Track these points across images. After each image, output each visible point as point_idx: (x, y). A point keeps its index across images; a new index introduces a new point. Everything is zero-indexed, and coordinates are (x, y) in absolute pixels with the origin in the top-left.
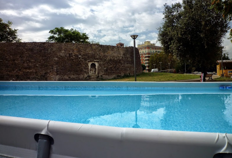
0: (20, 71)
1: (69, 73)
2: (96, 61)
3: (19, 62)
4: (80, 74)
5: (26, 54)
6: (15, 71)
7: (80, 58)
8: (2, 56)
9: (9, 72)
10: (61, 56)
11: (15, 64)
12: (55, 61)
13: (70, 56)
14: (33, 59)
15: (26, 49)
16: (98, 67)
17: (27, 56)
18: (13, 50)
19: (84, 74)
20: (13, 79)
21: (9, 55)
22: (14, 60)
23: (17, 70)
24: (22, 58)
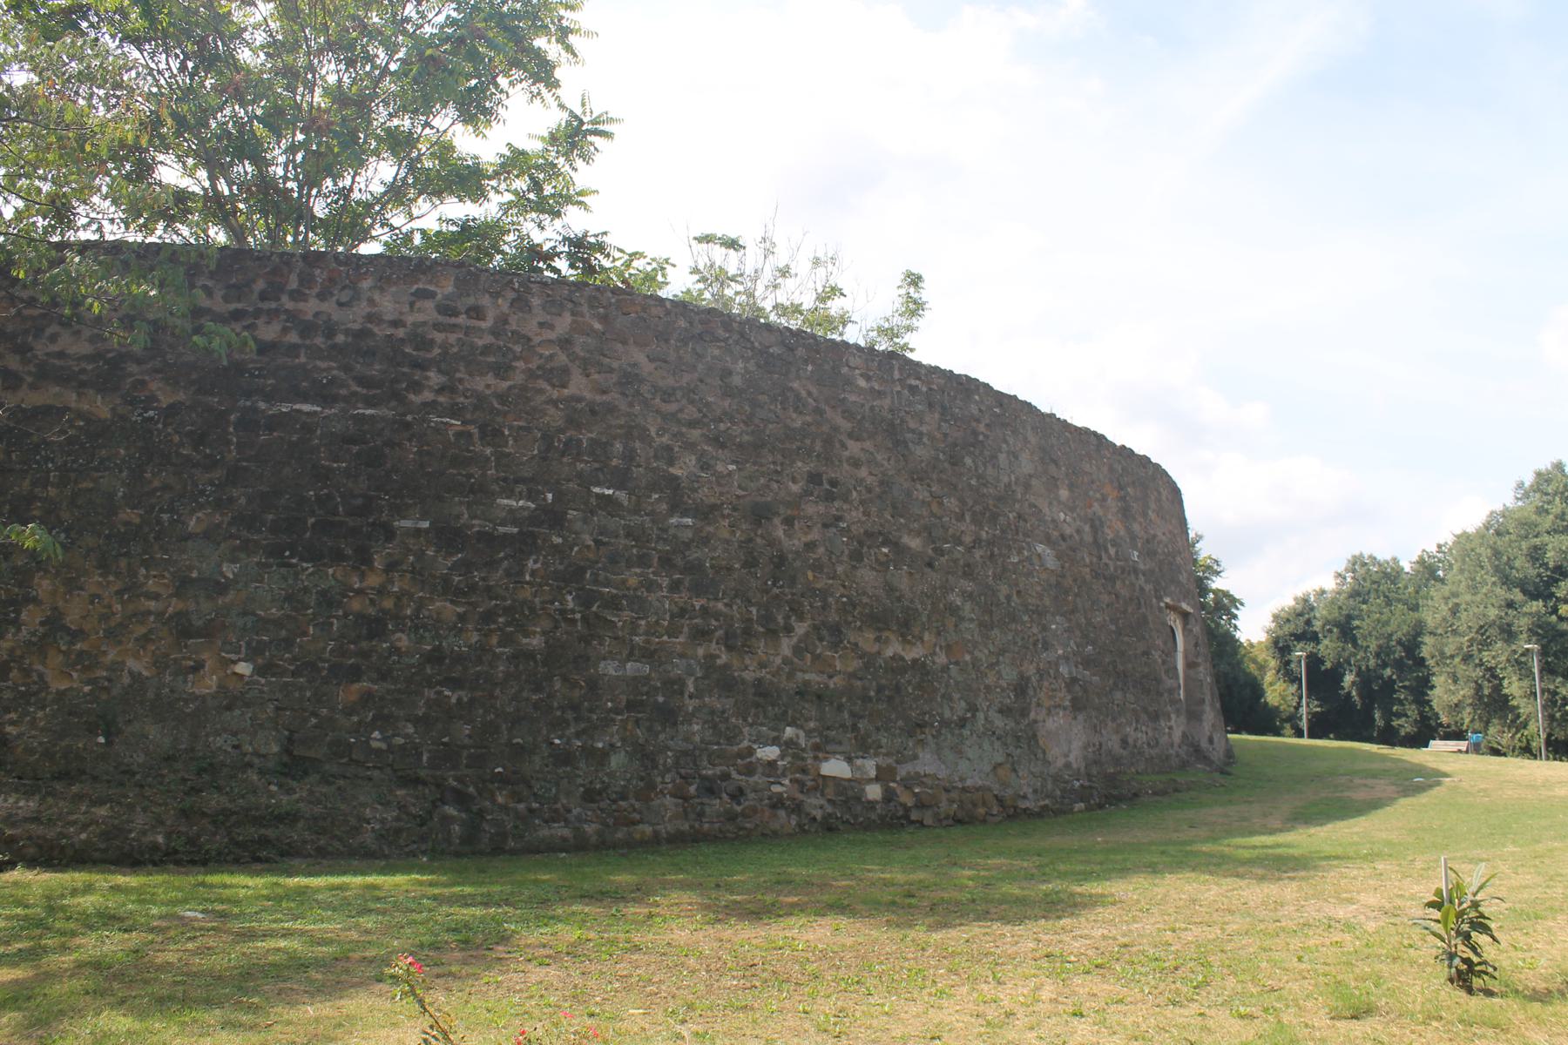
0: (835, 646)
1: (1118, 695)
2: (1184, 606)
3: (810, 546)
4: (1155, 717)
5: (856, 463)
6: (786, 646)
7: (1136, 571)
8: (618, 446)
9: (730, 648)
10: (1063, 537)
11: (780, 561)
12: (1044, 576)
13: (1095, 541)
14: (919, 534)
15: (848, 414)
16: (1190, 665)
17: (869, 490)
18: (728, 392)
19: (1169, 719)
20: (789, 732)
21: (690, 446)
22: (760, 515)
23: (801, 628)
24: (829, 497)
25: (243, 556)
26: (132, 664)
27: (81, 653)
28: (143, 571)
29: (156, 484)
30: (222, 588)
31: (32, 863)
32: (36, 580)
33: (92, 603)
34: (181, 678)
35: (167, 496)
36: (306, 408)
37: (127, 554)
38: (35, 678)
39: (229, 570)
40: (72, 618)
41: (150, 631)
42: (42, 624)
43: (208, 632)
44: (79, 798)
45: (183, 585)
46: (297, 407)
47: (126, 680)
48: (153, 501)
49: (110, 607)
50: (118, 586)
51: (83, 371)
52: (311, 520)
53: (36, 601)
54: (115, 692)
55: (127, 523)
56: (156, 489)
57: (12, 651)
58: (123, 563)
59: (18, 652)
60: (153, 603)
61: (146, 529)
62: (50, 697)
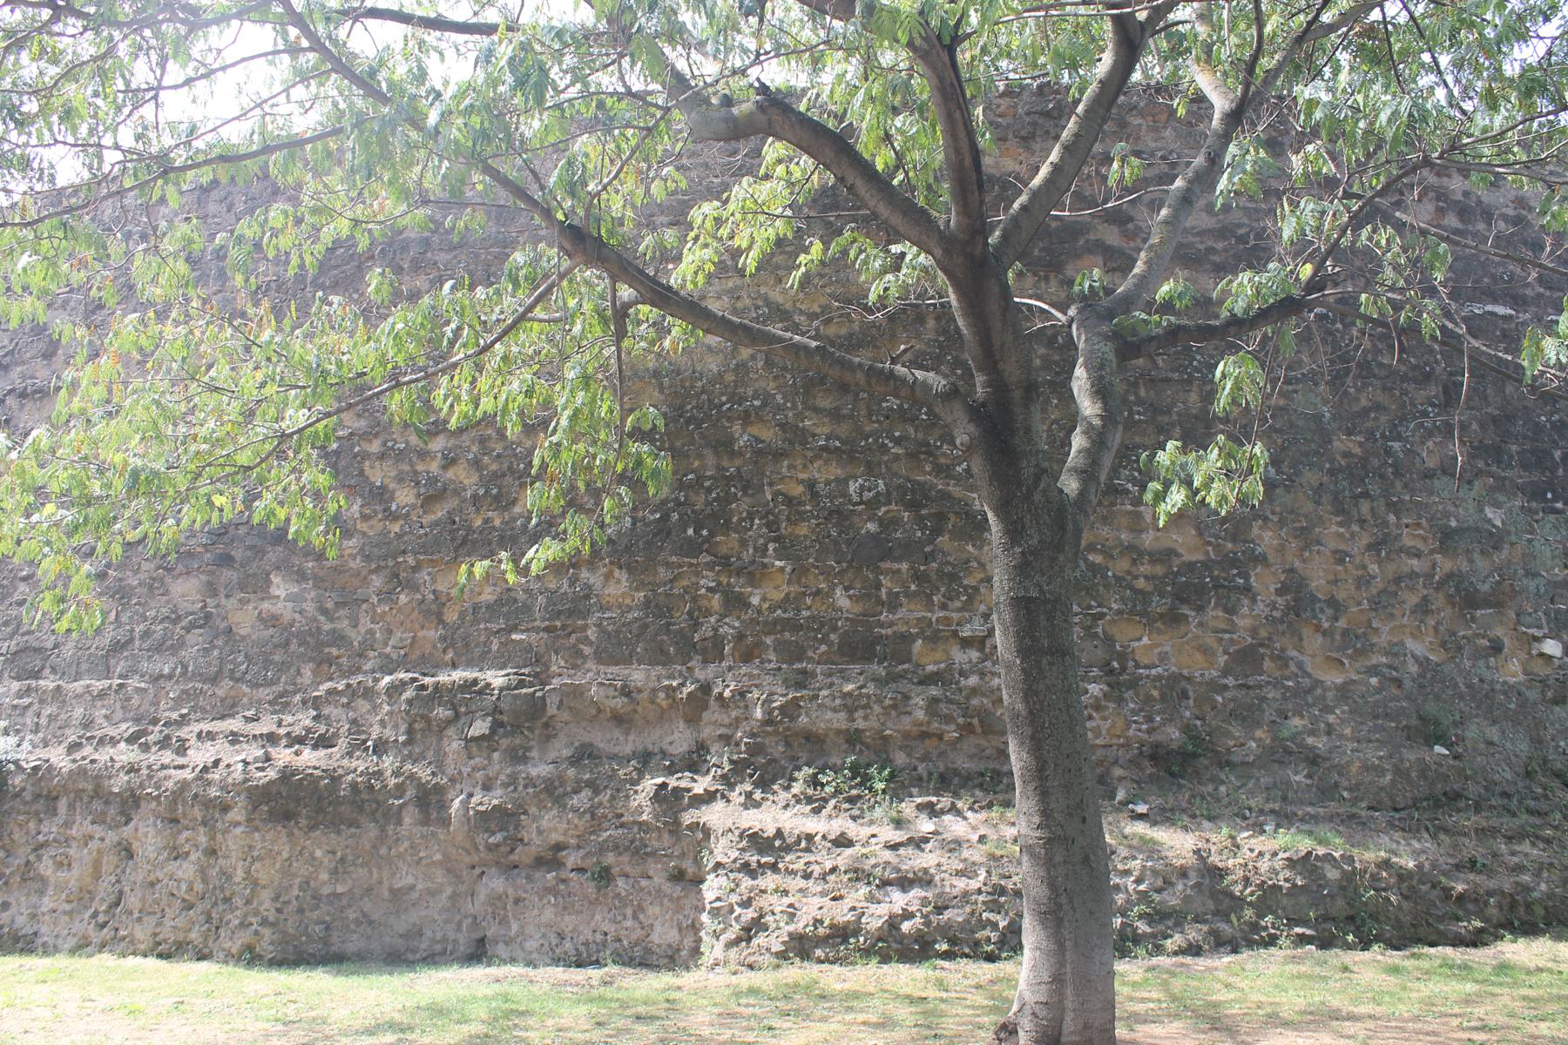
25: (1501, 498)
26: (1415, 646)
27: (1345, 633)
28: (1392, 518)
29: (1364, 402)
30: (1494, 540)
31: (1529, 930)
32: (1256, 531)
33: (1341, 561)
34: (1481, 663)
35: (1383, 419)
36: (1501, 310)
37: (1366, 495)
38: (1293, 668)
39: (1495, 516)
40: (1318, 582)
41: (1425, 598)
42: (1279, 592)
43: (1496, 601)
44: (1482, 833)
45: (1447, 539)
46: (1489, 308)
47: (1414, 669)
48: (1369, 424)
49: (1364, 567)
50: (1365, 540)
51: (1211, 250)
52: (1557, 454)
53: (1262, 560)
54: (1408, 684)
55: (1347, 455)
56: (1365, 412)
57: (1254, 631)
58: (1365, 506)
59: (1263, 633)
60: (1415, 562)
61: (1376, 463)
62: (1330, 695)
